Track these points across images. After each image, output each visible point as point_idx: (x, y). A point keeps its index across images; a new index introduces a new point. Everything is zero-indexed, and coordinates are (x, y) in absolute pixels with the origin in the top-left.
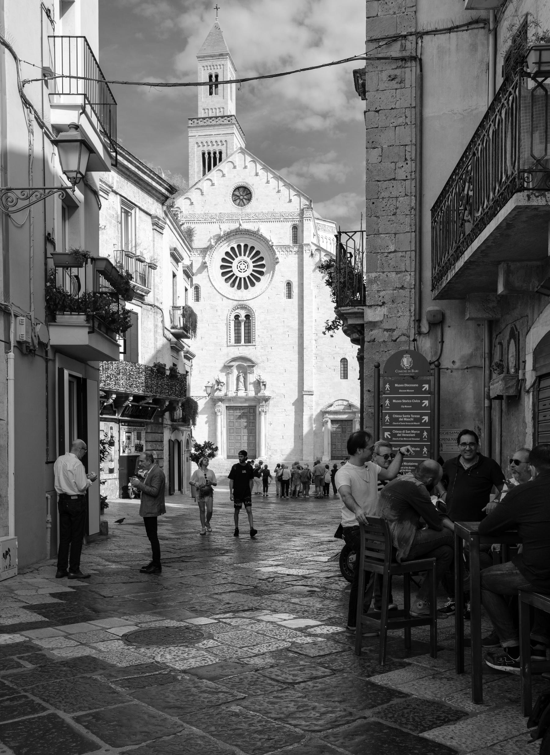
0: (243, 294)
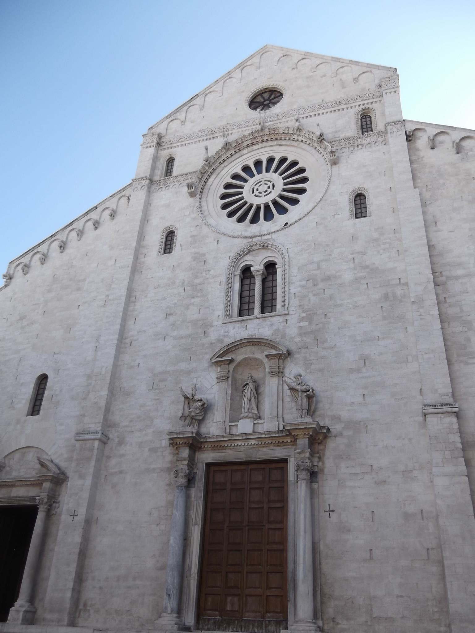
0: (263, 226)
